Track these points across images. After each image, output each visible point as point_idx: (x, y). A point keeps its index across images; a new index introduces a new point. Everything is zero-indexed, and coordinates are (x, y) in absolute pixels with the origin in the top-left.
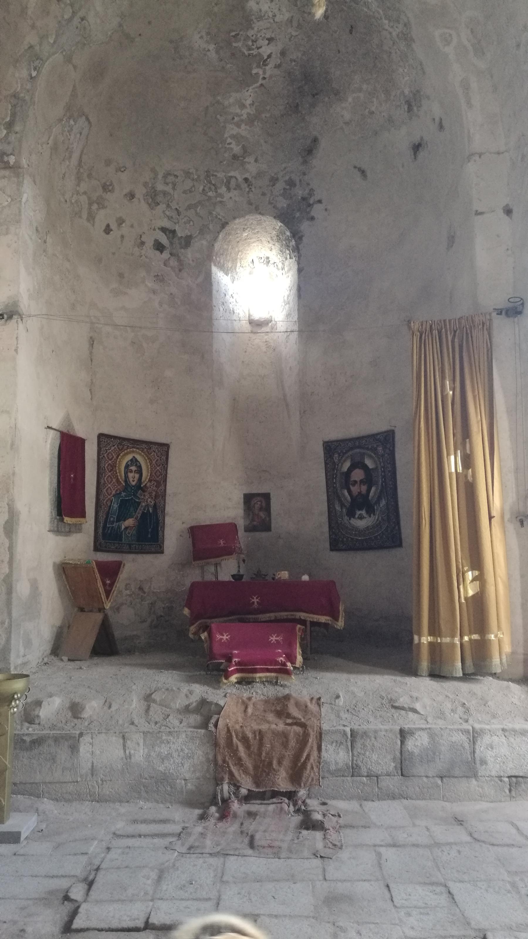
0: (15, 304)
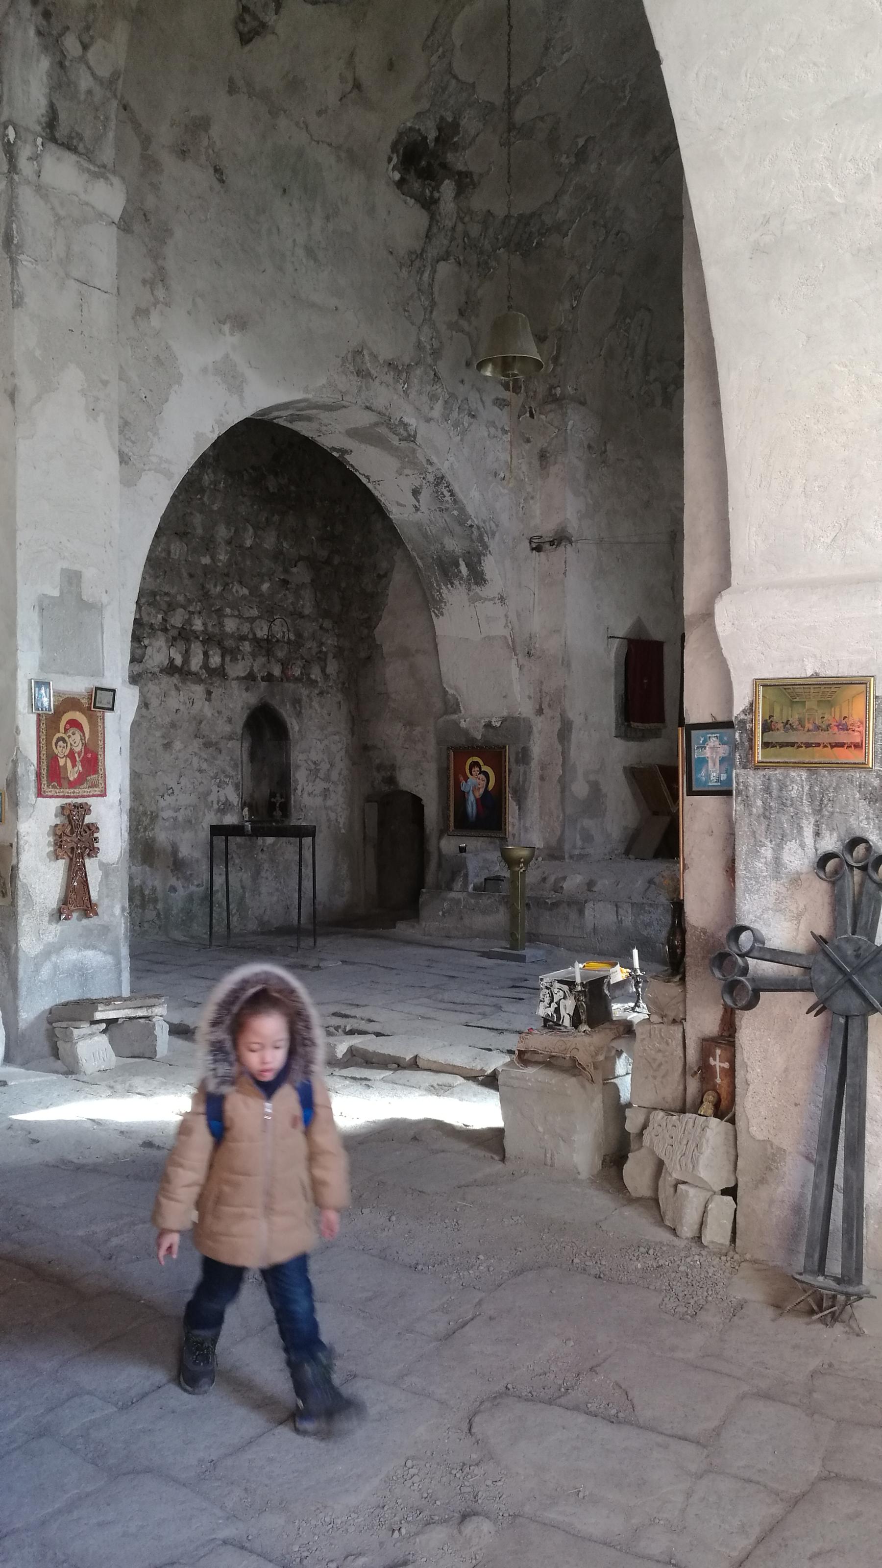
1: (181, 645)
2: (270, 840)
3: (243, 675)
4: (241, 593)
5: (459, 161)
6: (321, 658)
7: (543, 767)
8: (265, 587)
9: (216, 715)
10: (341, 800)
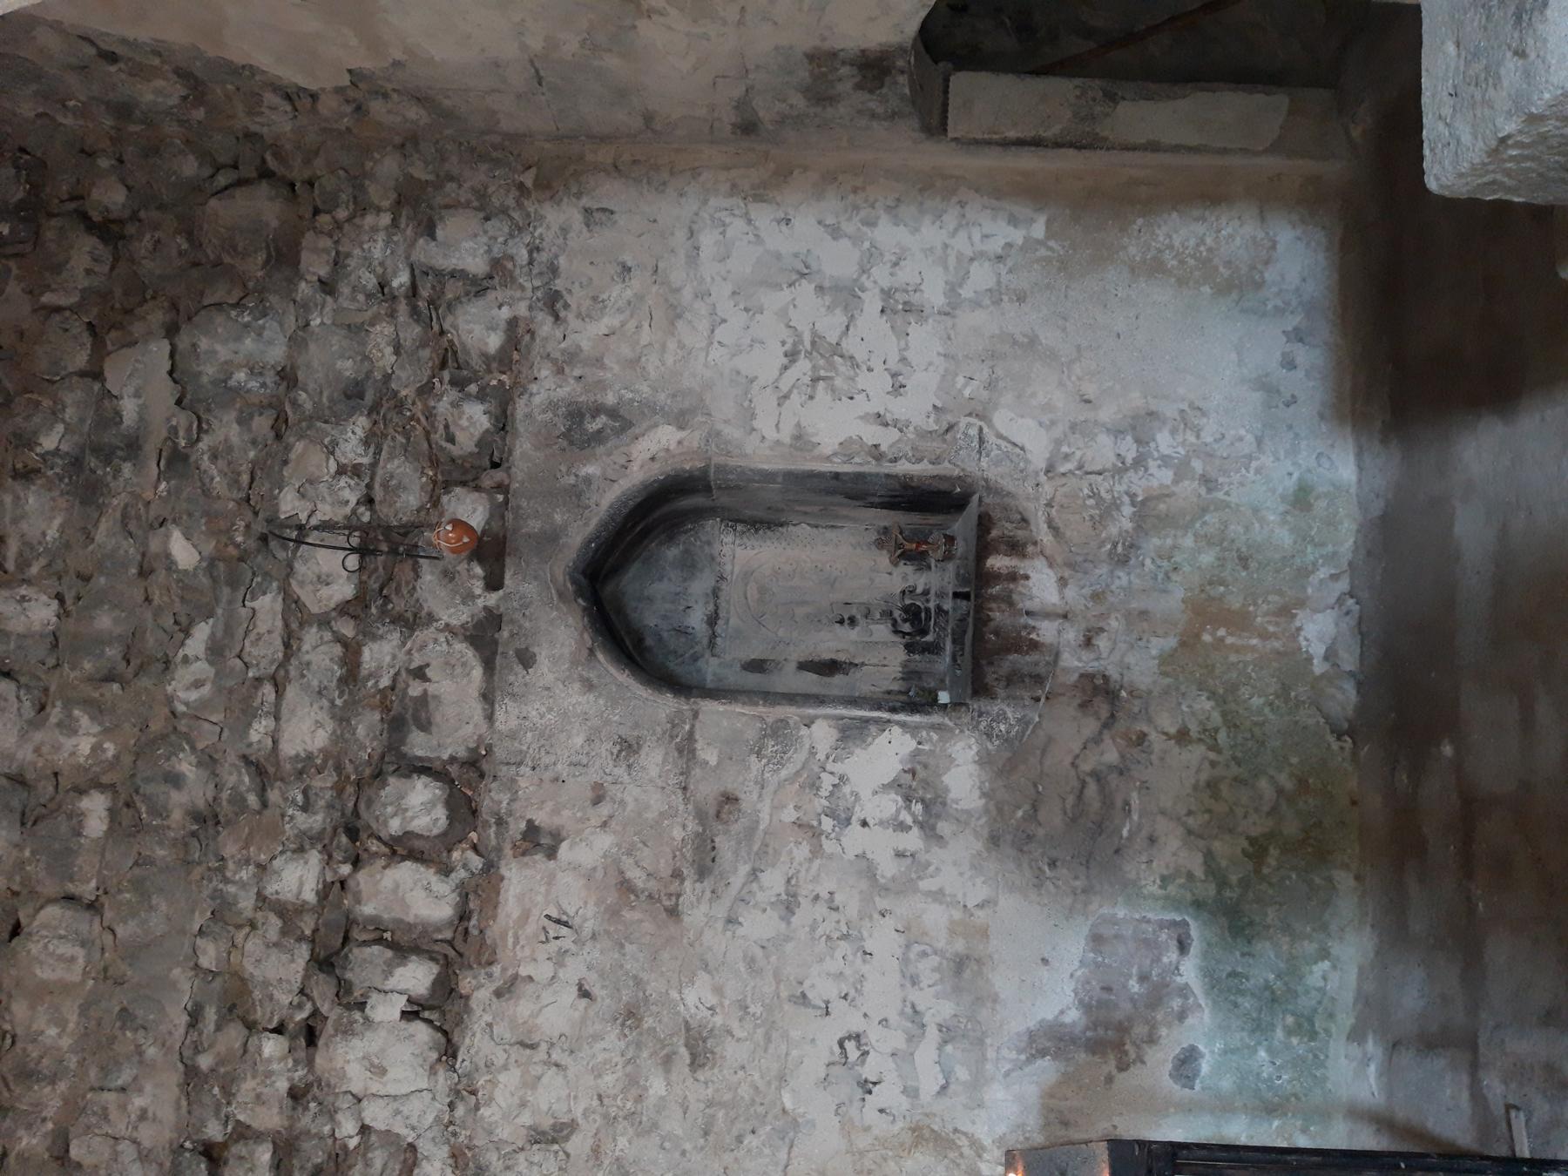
1: (366, 962)
2: (1042, 585)
3: (477, 673)
4: (202, 668)
6: (429, 298)
8: (183, 551)
9: (605, 810)
10: (931, 233)
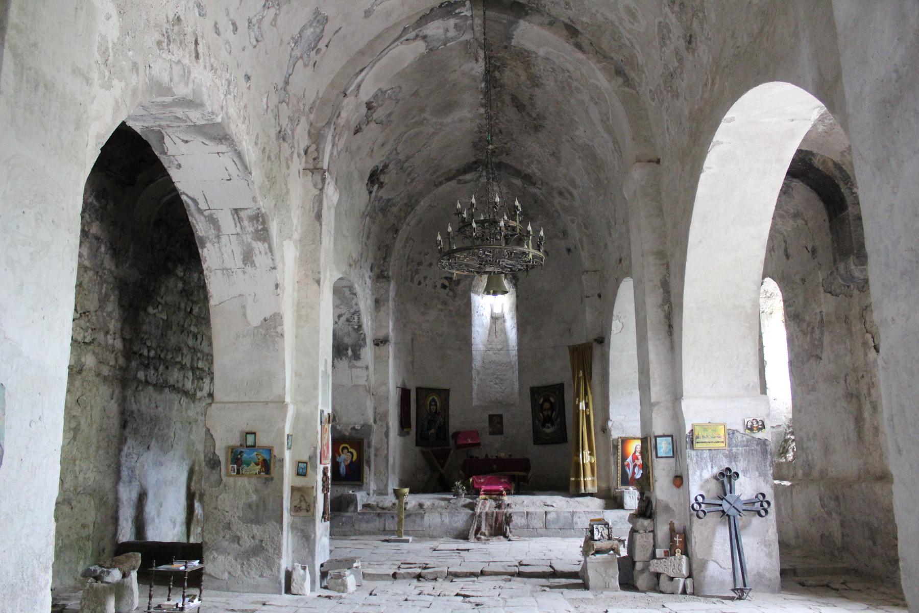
0: (388, 337)
5: (382, 178)
7: (377, 450)
